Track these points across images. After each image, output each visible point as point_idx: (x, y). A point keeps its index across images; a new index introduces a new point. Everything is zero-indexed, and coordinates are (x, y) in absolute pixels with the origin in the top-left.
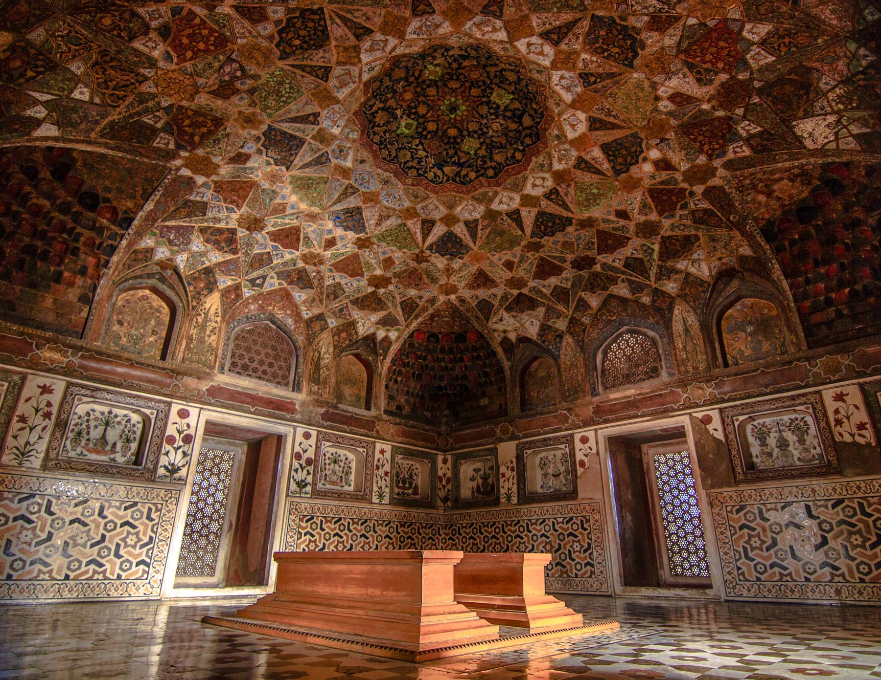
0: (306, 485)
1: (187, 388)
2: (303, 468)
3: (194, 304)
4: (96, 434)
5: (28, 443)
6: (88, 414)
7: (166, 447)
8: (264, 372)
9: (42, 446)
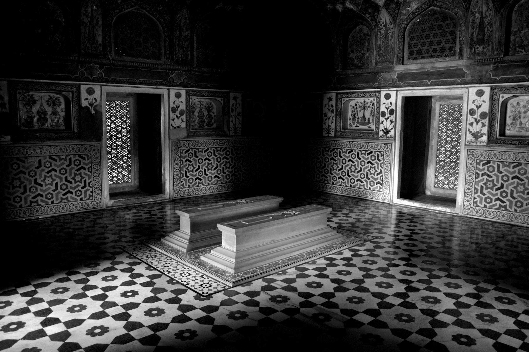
0: (482, 135)
1: (386, 81)
2: (477, 122)
3: (374, 24)
4: (360, 115)
5: (329, 125)
6: (356, 105)
7: (382, 119)
8: (435, 50)
9: (333, 126)
